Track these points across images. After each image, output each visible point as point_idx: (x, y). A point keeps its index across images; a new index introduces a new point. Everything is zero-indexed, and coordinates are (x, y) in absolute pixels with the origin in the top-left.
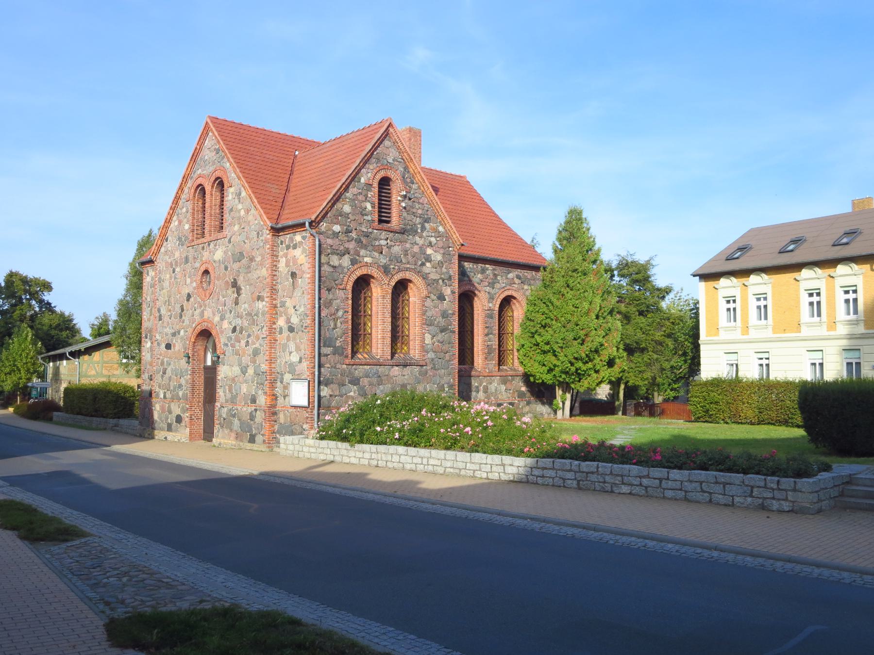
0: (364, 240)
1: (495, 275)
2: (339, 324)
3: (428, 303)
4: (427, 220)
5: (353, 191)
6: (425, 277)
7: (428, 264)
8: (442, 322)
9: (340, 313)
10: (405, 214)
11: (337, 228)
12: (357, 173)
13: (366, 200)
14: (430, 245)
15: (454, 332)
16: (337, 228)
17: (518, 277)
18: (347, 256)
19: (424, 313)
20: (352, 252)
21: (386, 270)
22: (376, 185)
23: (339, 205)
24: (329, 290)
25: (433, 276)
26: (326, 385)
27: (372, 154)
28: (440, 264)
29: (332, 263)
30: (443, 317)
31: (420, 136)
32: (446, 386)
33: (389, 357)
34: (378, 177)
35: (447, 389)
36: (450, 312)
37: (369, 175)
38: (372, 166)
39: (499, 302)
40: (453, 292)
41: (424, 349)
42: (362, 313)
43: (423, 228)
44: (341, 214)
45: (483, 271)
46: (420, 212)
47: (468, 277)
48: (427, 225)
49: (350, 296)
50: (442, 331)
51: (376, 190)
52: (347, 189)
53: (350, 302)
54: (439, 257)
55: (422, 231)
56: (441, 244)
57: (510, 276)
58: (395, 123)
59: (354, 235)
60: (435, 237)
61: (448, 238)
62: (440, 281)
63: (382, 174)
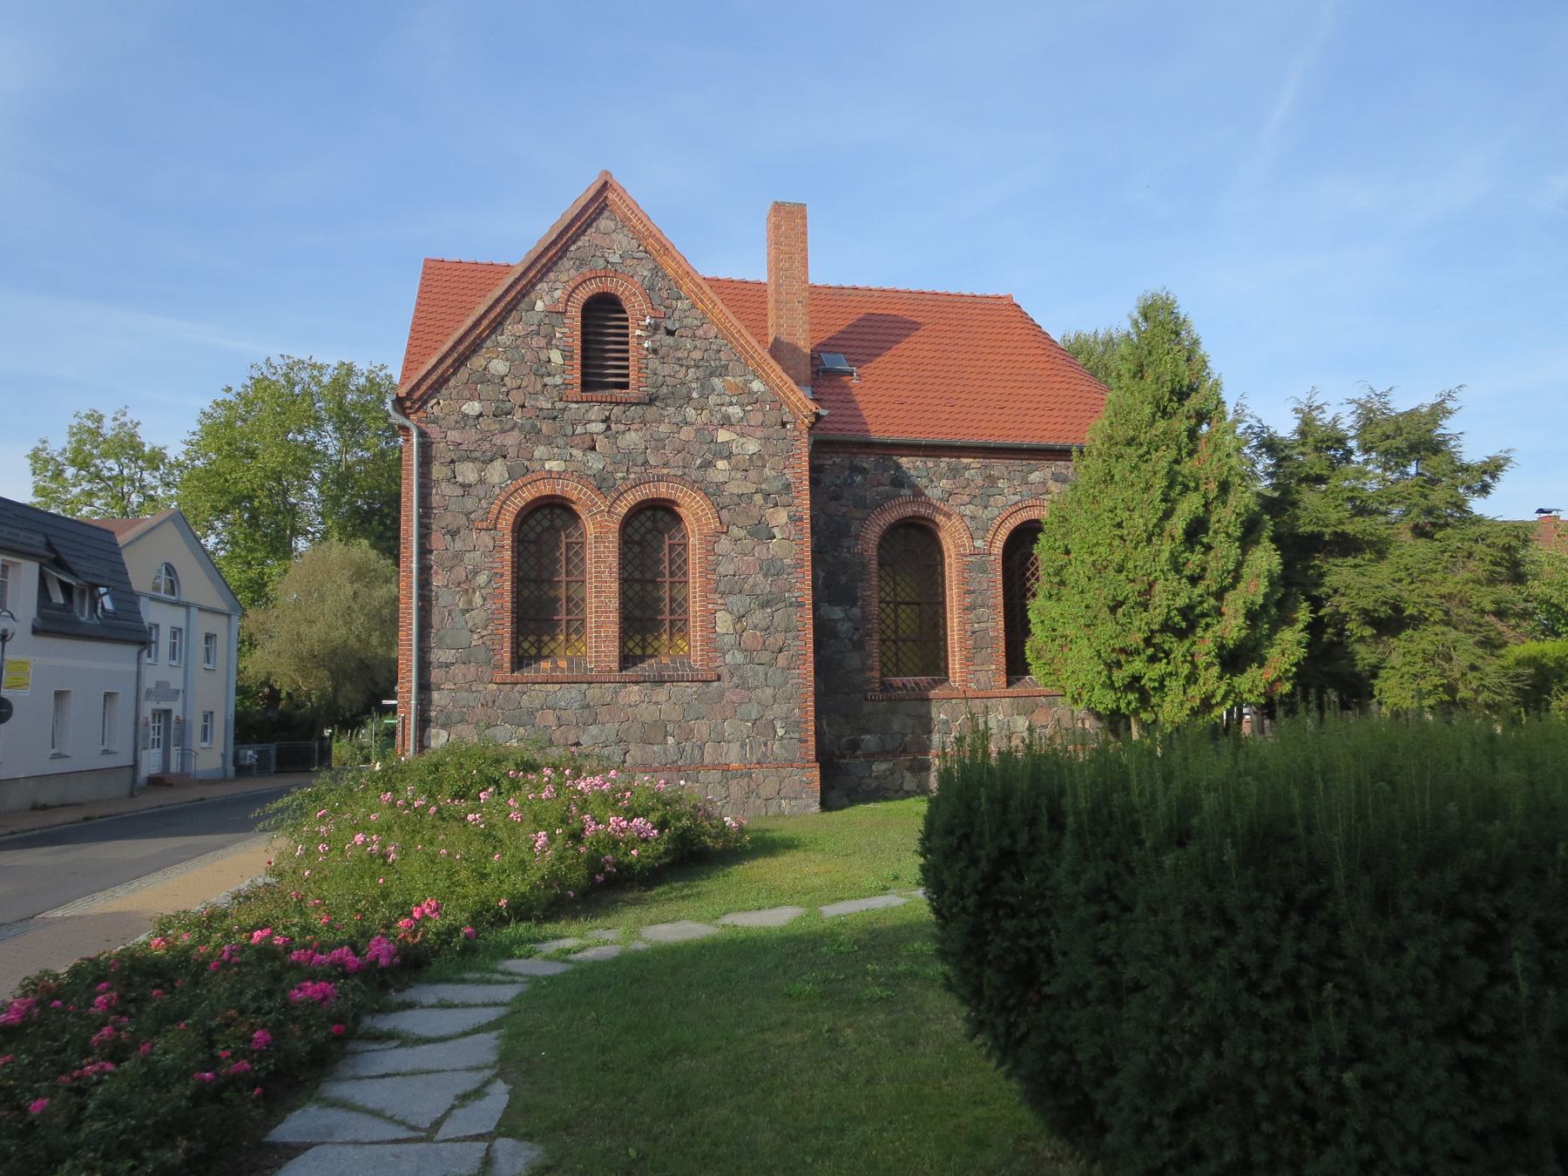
0: (546, 427)
1: (992, 480)
2: (478, 600)
3: (724, 545)
4: (722, 371)
5: (512, 328)
6: (713, 493)
7: (721, 464)
8: (763, 584)
9: (482, 579)
10: (654, 363)
11: (473, 408)
12: (523, 294)
13: (549, 345)
14: (726, 422)
15: (801, 605)
16: (473, 408)
17: (1057, 478)
18: (499, 462)
19: (710, 568)
20: (512, 453)
21: (602, 484)
22: (575, 312)
23: (477, 362)
24: (454, 534)
25: (733, 488)
26: (443, 727)
27: (564, 250)
28: (757, 460)
29: (460, 479)
30: (765, 576)
31: (804, 218)
32: (778, 724)
33: (615, 666)
34: (582, 295)
35: (781, 732)
36: (788, 561)
37: (558, 294)
38: (566, 274)
39: (1003, 534)
40: (795, 519)
41: (710, 642)
42: (563, 577)
43: (706, 390)
44: (484, 377)
45: (954, 473)
46: (697, 355)
47: (913, 486)
48: (716, 381)
49: (508, 542)
50: (763, 606)
51: (578, 322)
52: (497, 325)
53: (508, 554)
54: (752, 447)
55: (704, 396)
56: (756, 418)
57: (1035, 477)
58: (620, 179)
59: (518, 417)
60: (742, 405)
61: (778, 404)
62: (758, 498)
63: (593, 288)
